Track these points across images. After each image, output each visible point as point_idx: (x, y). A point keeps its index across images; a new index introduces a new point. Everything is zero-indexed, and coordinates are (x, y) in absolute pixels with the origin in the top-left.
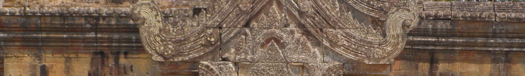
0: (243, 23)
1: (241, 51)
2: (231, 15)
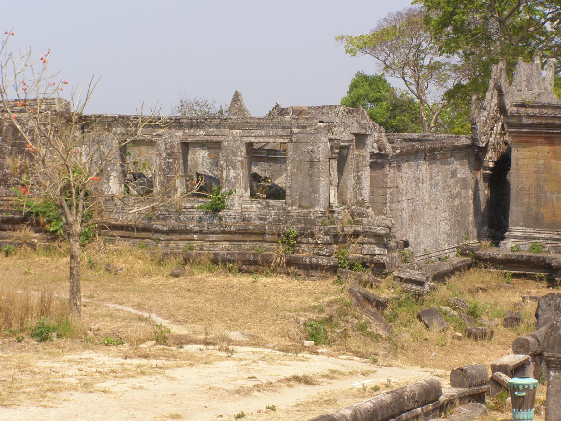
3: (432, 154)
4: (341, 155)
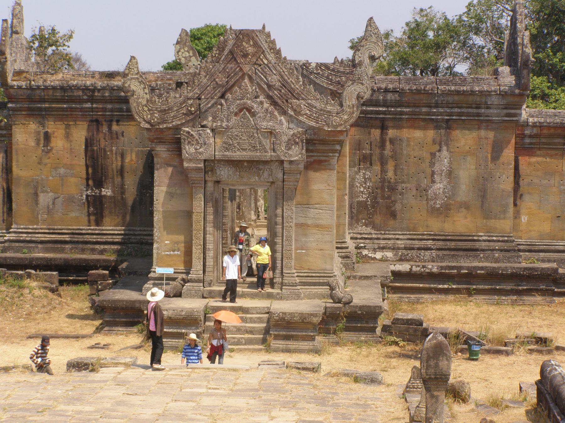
0: (219, 95)
1: (218, 119)
2: (208, 88)
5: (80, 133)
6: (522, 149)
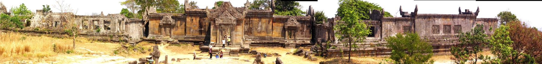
3: (136, 22)
4: (120, 22)
5: (198, 19)
6: (273, 22)
